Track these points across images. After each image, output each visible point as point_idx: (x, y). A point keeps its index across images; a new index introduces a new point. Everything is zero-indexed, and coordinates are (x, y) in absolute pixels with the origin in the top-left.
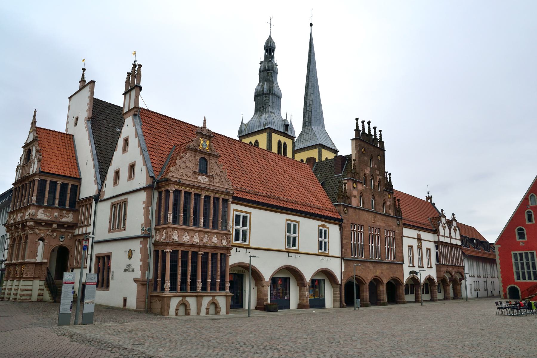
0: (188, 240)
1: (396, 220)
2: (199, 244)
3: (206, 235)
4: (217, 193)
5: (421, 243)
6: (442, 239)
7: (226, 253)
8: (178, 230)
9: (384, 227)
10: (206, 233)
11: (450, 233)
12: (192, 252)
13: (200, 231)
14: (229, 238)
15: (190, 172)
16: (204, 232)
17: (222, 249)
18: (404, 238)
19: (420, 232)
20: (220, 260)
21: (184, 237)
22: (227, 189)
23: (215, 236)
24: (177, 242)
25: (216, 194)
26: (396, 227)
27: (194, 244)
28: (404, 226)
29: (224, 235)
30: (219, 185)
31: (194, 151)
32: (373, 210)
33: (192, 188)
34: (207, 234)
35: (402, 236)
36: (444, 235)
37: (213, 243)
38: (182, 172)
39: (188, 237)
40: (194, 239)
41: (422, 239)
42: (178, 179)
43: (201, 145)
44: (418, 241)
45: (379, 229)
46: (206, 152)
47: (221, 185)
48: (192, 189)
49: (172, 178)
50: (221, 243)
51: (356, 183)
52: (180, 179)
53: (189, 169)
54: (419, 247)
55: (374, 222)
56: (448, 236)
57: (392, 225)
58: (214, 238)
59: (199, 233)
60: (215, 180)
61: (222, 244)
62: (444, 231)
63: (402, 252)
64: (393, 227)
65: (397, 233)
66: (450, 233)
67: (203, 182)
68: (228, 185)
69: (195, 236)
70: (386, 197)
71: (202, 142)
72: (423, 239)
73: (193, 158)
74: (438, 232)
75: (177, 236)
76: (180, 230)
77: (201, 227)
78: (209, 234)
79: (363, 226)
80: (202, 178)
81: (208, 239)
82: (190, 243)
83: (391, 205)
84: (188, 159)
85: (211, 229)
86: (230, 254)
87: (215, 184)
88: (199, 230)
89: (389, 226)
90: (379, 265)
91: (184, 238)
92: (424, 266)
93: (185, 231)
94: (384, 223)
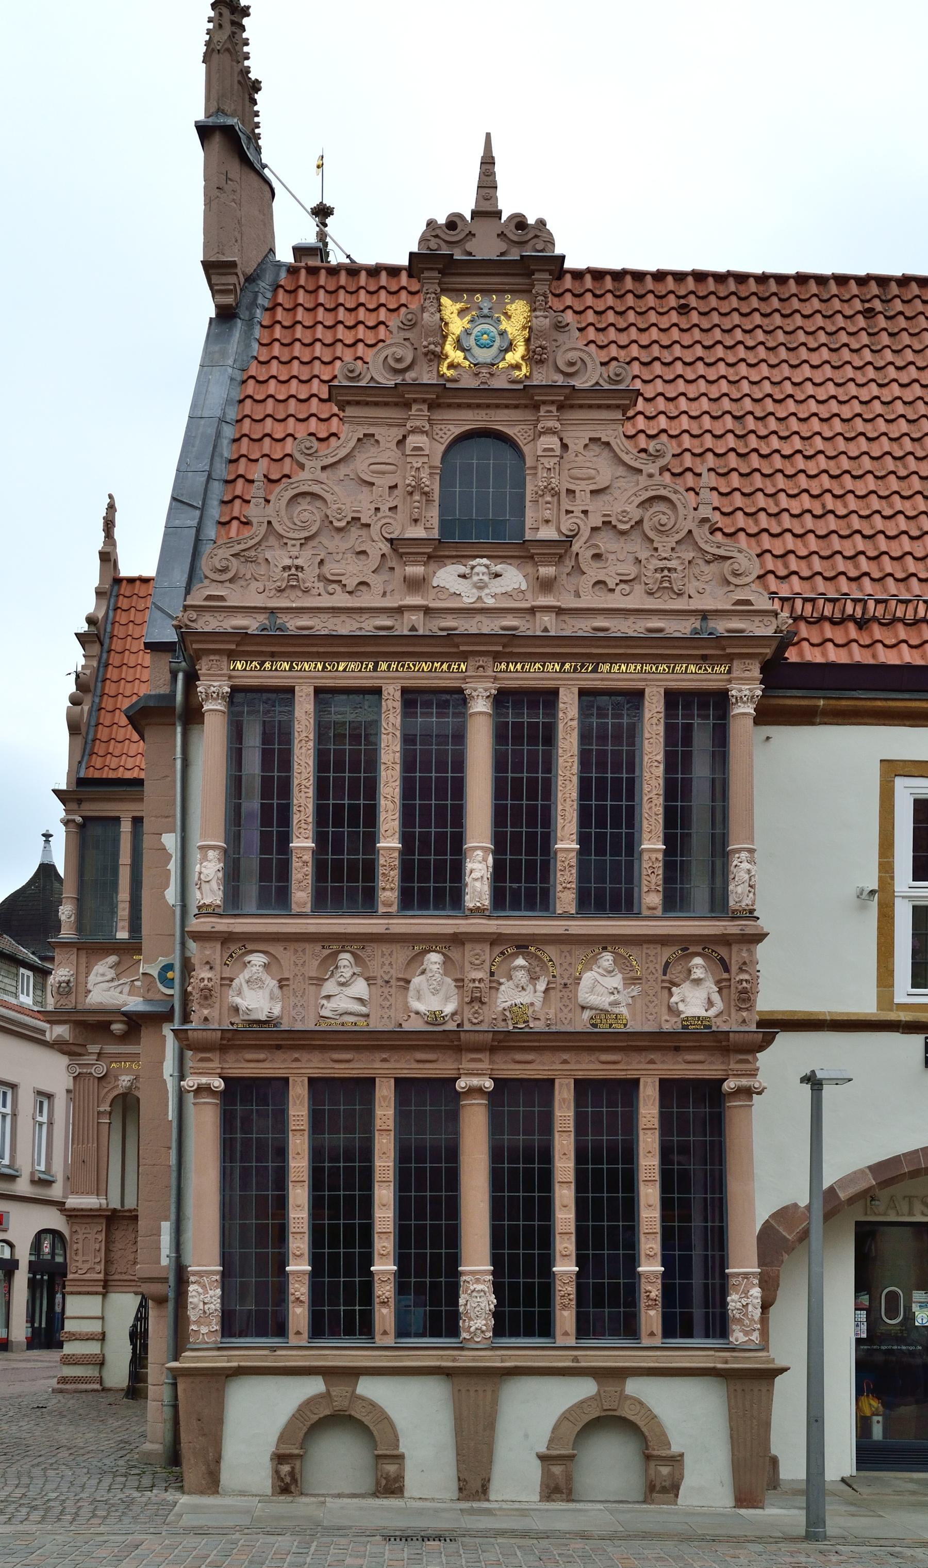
0: (364, 1010)
2: (451, 1026)
3: (520, 961)
4: (613, 659)
7: (718, 1075)
8: (277, 949)
10: (522, 944)
12: (401, 1084)
13: (458, 940)
14: (734, 968)
15: (364, 552)
16: (495, 940)
17: (677, 1049)
20: (656, 1123)
21: (330, 987)
22: (704, 615)
23: (607, 959)
24: (259, 1022)
25: (605, 668)
27: (407, 1027)
29: (692, 949)
30: (636, 599)
31: (396, 404)
33: (376, 658)
34: (527, 956)
37: (587, 1015)
38: (288, 562)
39: (360, 988)
40: (412, 992)
42: (262, 618)
43: (449, 348)
46: (499, 383)
47: (650, 593)
48: (384, 666)
49: (207, 617)
50: (664, 1010)
52: (272, 611)
53: (355, 532)
58: (588, 977)
59: (455, 954)
60: (594, 572)
61: (673, 1011)
67: (480, 598)
68: (729, 583)
69: (423, 972)
71: (457, 326)
73: (387, 452)
75: (272, 983)
76: (292, 946)
77: (478, 912)
78: (552, 951)
80: (463, 576)
81: (541, 986)
82: (376, 1024)
84: (343, 470)
85: (570, 917)
86: (744, 1082)
87: (590, 600)
88: (450, 930)
91: (328, 997)
93: (335, 947)
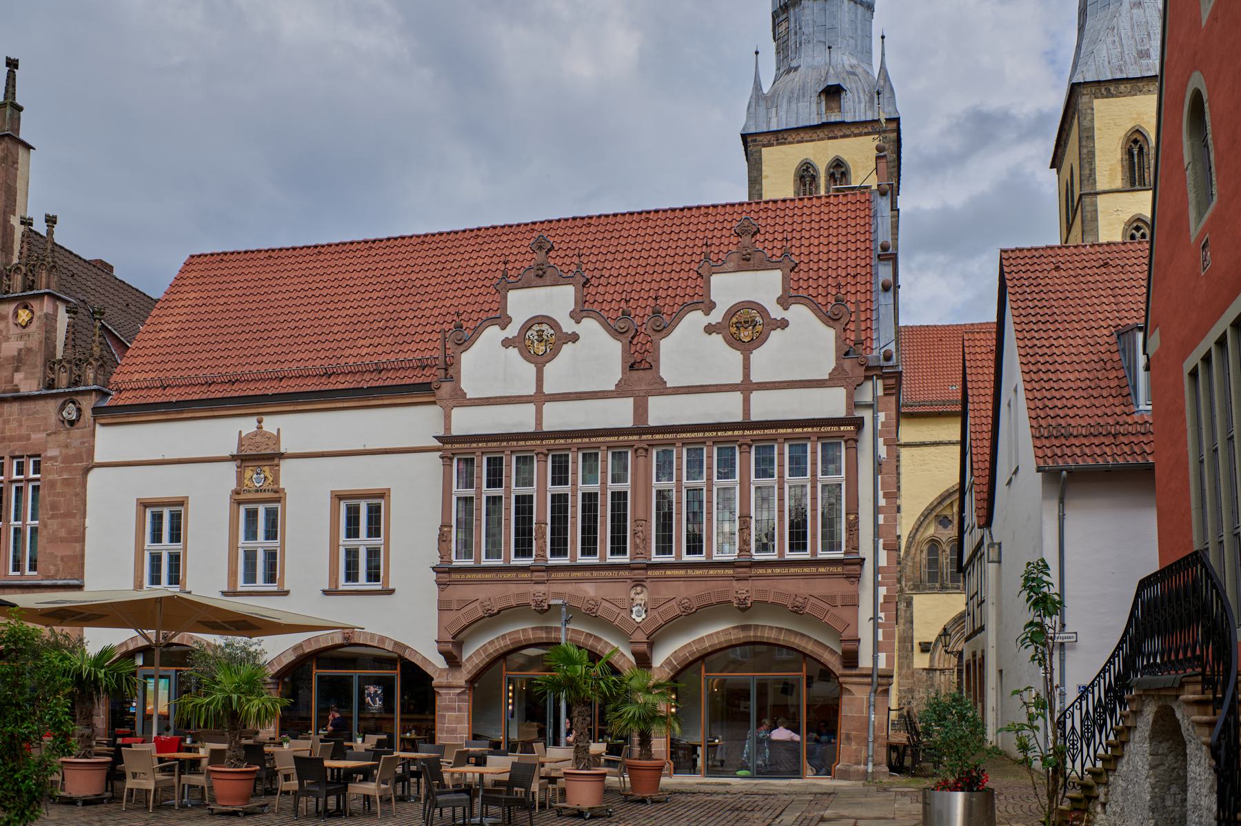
1: (52, 406)
19: (266, 419)
41: (282, 456)
57: (24, 431)
65: (51, 458)
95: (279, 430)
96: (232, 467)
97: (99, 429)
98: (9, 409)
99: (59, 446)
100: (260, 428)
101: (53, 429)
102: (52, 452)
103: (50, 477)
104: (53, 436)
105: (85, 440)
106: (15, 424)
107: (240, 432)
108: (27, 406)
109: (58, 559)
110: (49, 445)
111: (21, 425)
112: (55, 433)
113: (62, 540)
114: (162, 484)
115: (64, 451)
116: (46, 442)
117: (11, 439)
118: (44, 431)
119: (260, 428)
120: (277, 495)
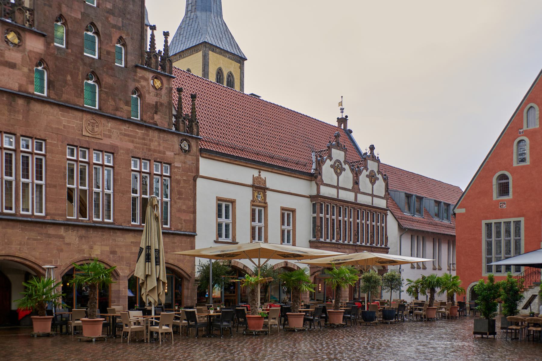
1: (176, 140)
5: (265, 196)
6: (325, 191)
9: (128, 151)
11: (356, 183)
18: (199, 181)
26: (175, 154)
28: (202, 155)
32: (96, 110)
35: (197, 176)
36: (336, 185)
41: (268, 189)
44: (253, 190)
45: (113, 153)
51: (22, 34)
54: (255, 203)
55: (88, 135)
56: (350, 186)
57: (161, 148)
62: (373, 185)
63: (192, 210)
64: (164, 153)
65: (177, 167)
66: (356, 183)
70: (143, 83)
72: (270, 188)
74: (316, 177)
79: (45, 140)
83: (162, 104)
89: (150, 150)
90: (103, 235)
92: (237, 241)
94: (133, 142)
95: (265, 178)
96: (250, 190)
97: (202, 160)
98: (152, 133)
99: (181, 162)
100: (260, 175)
101: (177, 152)
102: (176, 165)
103: (177, 177)
104: (177, 156)
105: (194, 162)
106: (156, 144)
107: (253, 175)
108: (162, 135)
109: (183, 221)
110: (175, 160)
111: (159, 145)
112: (178, 154)
113: (184, 211)
114: (228, 192)
115: (183, 165)
116: (174, 158)
117: (155, 151)
118: (173, 151)
119: (260, 175)
120: (265, 205)
